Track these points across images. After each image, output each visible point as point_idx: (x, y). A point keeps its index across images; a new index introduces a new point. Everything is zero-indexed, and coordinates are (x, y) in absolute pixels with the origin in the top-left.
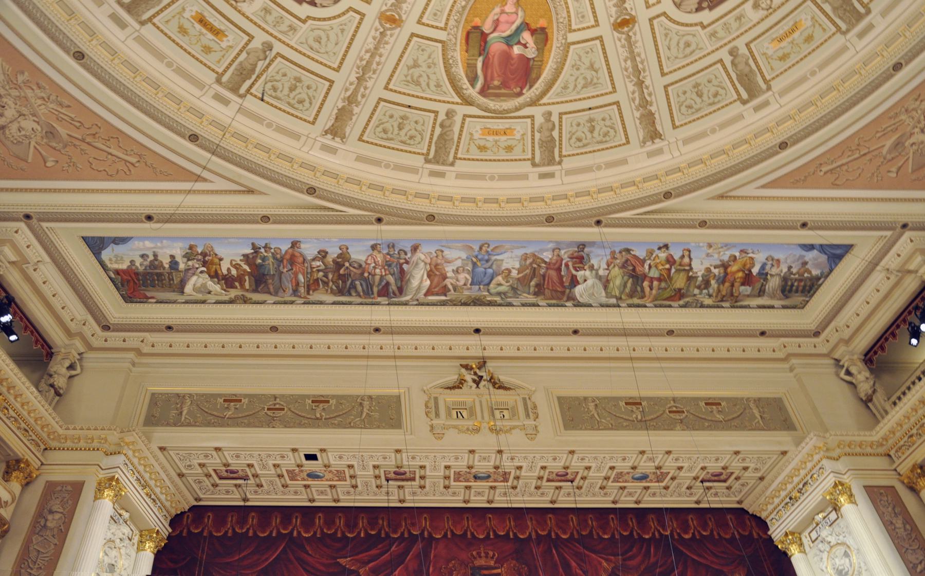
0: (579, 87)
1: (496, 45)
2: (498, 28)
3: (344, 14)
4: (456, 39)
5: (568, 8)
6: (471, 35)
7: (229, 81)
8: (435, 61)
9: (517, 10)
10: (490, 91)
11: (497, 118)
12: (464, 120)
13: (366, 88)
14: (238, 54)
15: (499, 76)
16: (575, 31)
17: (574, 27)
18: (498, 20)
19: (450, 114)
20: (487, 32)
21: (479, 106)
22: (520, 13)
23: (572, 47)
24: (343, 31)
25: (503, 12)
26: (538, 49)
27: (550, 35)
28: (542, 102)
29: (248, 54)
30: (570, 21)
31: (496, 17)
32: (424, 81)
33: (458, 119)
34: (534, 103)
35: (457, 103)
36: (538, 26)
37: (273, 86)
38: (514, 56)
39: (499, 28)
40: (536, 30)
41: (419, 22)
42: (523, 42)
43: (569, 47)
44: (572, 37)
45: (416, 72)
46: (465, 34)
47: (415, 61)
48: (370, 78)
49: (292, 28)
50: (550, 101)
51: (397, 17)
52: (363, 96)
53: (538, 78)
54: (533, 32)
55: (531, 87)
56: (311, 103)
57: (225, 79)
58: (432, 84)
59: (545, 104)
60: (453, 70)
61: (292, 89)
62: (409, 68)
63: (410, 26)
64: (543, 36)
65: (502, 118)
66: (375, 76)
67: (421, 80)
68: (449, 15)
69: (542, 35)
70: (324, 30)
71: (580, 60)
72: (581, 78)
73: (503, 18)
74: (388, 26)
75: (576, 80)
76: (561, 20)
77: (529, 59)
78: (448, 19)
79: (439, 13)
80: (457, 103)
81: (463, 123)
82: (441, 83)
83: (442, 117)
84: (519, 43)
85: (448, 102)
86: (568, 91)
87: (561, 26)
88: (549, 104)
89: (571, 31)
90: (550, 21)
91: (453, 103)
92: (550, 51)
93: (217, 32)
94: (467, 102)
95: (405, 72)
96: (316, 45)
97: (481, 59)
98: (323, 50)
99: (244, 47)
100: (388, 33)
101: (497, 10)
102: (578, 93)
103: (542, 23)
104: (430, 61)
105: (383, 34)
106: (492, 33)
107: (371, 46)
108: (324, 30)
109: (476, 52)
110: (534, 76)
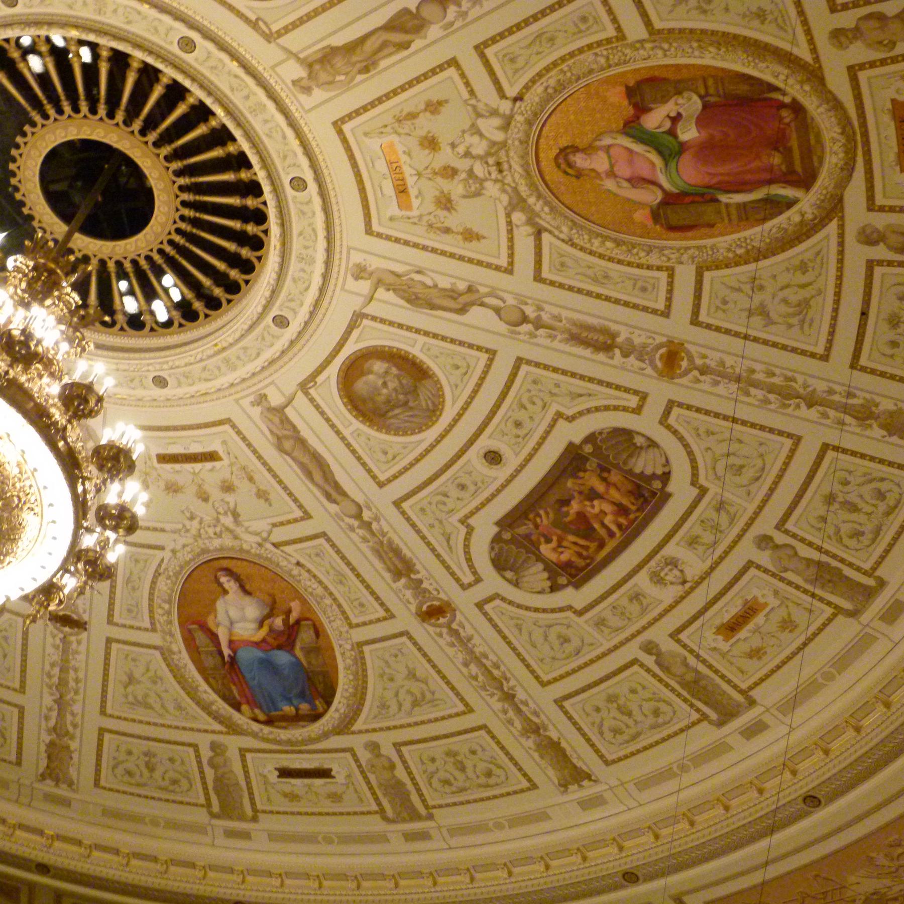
1: (689, 174)
3: (675, 432)
4: (687, 248)
5: (572, 55)
7: (851, 599)
8: (744, 278)
9: (600, 148)
10: (799, 169)
11: (866, 143)
12: (882, 209)
13: (831, 392)
14: (790, 583)
15: (758, 157)
16: (619, 29)
17: (611, 32)
18: (629, 180)
19: (870, 238)
20: (659, 196)
22: (607, 141)
23: (658, 24)
24: (709, 433)
26: (679, 93)
27: (644, 75)
28: (807, 57)
29: (786, 570)
30: (599, 44)
31: (626, 184)
32: (795, 296)
33: (880, 221)
34: (814, 75)
35: (841, 227)
36: (625, 102)
37: (851, 537)
38: (705, 135)
39: (646, 174)
40: (636, 106)
41: (666, 313)
42: (668, 124)
43: (660, 32)
44: (635, 30)
45: (776, 310)
46: (672, 235)
48: (805, 386)
49: (721, 506)
50: (802, 38)
51: (663, 350)
52: (849, 395)
54: (641, 109)
55: (776, 89)
56: (883, 480)
57: (847, 605)
58: (801, 278)
59: (814, 50)
61: (854, 508)
62: (769, 322)
63: (678, 327)
65: (865, 134)
66: (800, 379)
67: (794, 298)
68: (639, 266)
69: (643, 91)
70: (715, 461)
73: (624, 170)
74: (684, 364)
76: (602, 61)
77: (705, 106)
78: (649, 267)
79: (639, 284)
80: (841, 227)
81: (892, 209)
82: (796, 262)
83: (880, 252)
84: (672, 132)
85: (841, 244)
87: (614, 59)
88: (811, 41)
89: (621, 36)
91: (841, 235)
92: (678, 67)
93: (749, 611)
94: (834, 207)
96: (749, 473)
97: (724, 198)
98: (759, 463)
99: (774, 575)
101: (610, 184)
103: (617, 97)
105: (704, 370)
106: (660, 187)
107: (734, 387)
108: (715, 461)
109: (709, 209)
110: (743, 89)
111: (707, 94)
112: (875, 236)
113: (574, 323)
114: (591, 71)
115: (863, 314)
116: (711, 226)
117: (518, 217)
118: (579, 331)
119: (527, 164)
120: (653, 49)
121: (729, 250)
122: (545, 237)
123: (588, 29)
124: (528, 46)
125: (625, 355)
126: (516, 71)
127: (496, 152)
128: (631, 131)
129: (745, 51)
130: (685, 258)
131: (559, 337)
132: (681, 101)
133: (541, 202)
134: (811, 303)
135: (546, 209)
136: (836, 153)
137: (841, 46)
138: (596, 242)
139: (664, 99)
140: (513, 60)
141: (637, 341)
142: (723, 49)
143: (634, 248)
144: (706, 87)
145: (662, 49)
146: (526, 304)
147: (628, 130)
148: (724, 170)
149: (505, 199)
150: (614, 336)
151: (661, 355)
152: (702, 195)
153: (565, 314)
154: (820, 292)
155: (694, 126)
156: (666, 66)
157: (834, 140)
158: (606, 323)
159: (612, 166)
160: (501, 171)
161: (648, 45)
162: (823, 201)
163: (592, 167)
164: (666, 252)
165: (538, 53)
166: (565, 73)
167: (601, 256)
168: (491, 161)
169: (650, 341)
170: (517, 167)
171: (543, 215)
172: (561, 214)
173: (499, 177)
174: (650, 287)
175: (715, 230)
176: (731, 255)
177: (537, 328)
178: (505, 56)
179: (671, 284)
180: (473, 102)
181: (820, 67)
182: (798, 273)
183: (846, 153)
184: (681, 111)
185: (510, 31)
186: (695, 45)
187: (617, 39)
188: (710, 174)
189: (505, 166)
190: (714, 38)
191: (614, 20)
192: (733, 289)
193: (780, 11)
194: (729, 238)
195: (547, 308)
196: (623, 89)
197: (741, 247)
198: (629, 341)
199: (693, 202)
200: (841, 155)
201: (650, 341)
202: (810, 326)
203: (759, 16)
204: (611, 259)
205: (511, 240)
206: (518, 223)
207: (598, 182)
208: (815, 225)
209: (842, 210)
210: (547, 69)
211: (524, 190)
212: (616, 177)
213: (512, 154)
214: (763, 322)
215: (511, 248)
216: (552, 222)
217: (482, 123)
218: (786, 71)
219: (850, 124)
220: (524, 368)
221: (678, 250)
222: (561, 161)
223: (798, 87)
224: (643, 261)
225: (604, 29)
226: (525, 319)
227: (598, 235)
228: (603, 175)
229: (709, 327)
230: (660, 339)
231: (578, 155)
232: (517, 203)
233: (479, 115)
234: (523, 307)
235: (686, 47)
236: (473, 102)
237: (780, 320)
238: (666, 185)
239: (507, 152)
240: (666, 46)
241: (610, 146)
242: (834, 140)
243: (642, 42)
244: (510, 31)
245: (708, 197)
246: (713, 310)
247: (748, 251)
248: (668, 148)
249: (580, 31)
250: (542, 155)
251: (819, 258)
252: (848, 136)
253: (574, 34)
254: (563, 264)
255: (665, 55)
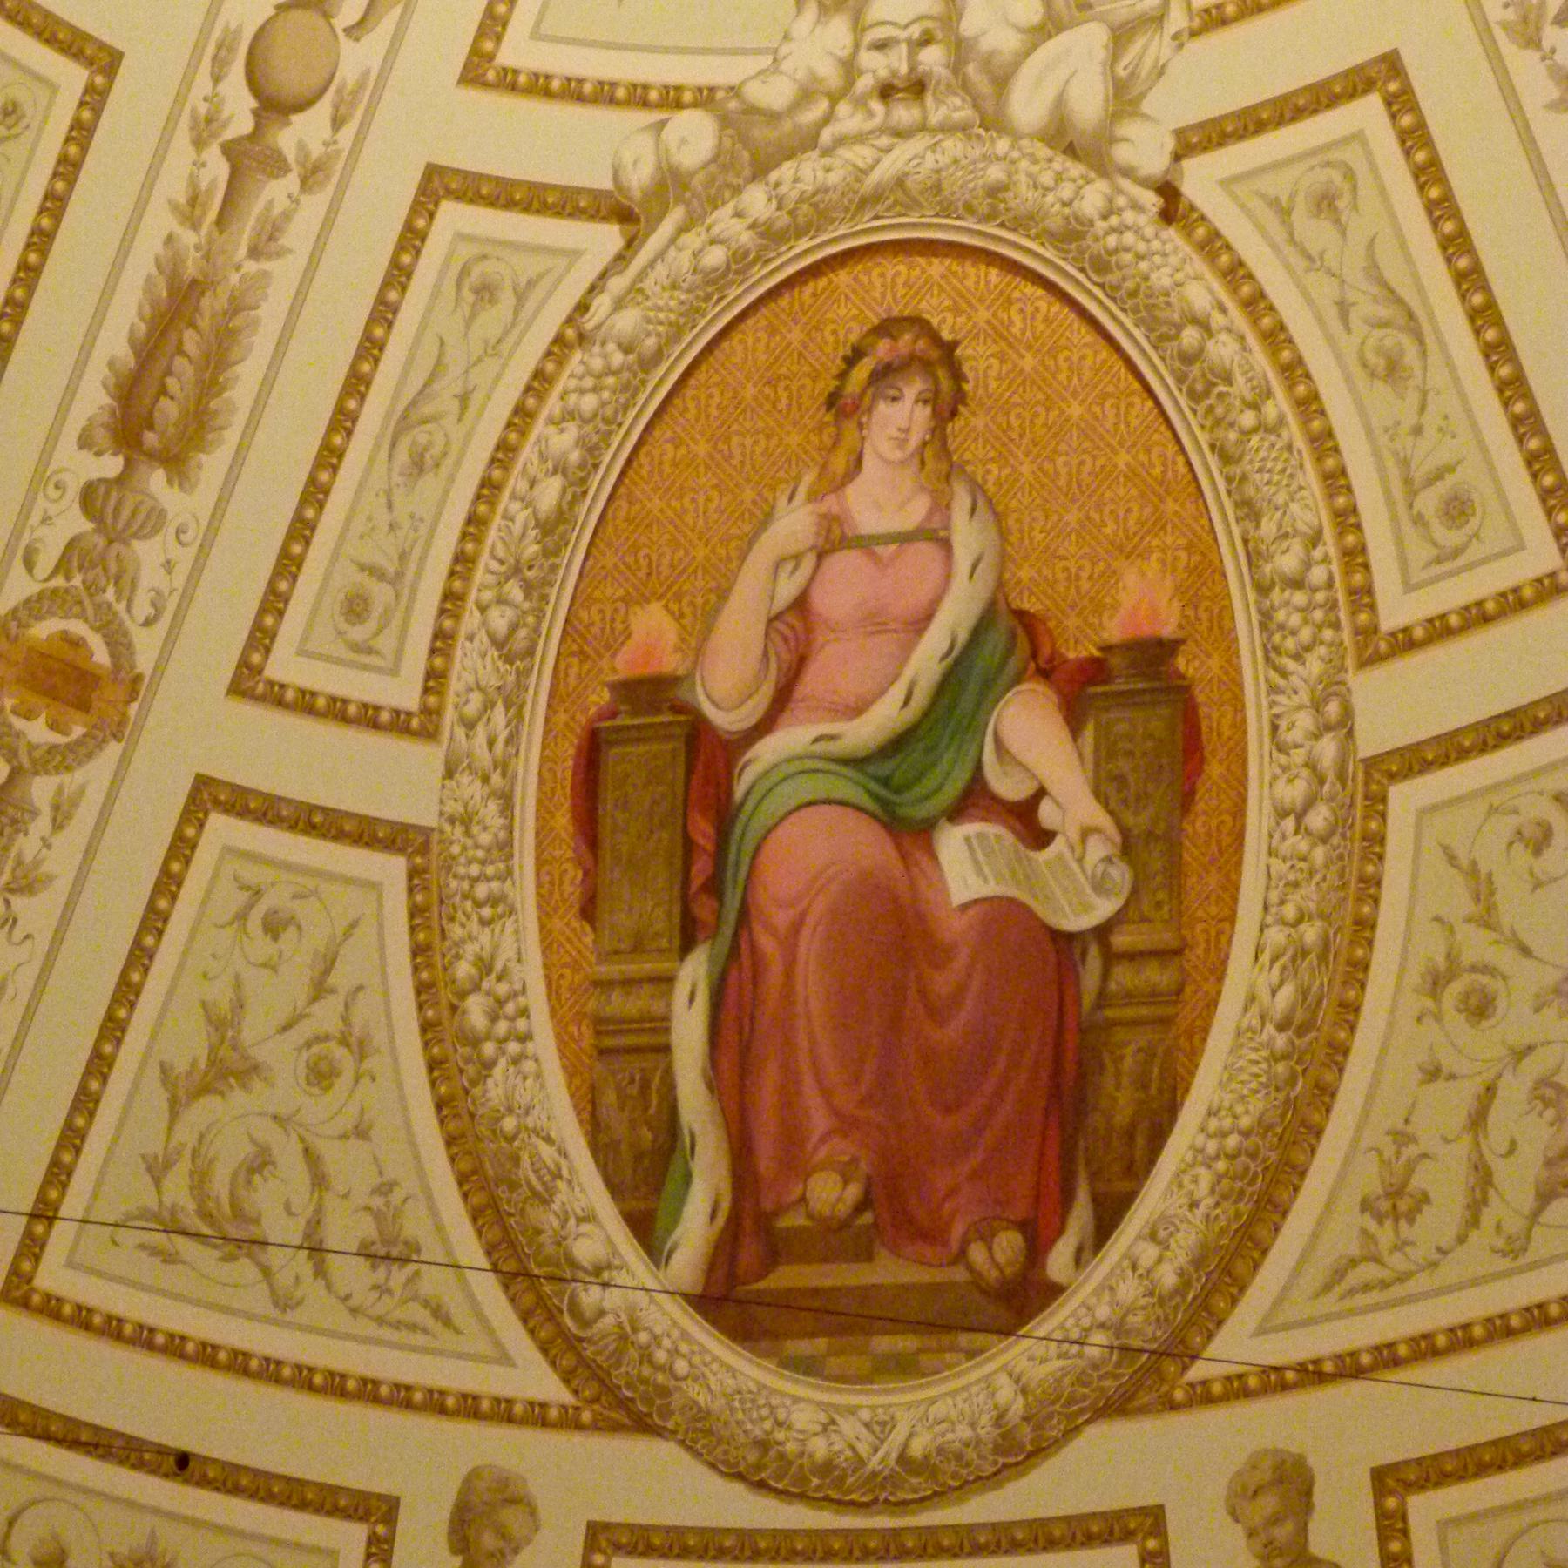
0: (1516, 1182)
1: (806, 851)
2: (812, 683)
4: (507, 801)
5: (1324, 442)
6: (616, 760)
9: (941, 506)
10: (787, 1277)
15: (846, 1125)
16: (1405, 643)
17: (1397, 609)
18: (801, 604)
20: (727, 721)
21: (704, 1438)
22: (969, 536)
23: (1405, 798)
25: (834, 538)
26: (1127, 847)
27: (1213, 718)
30: (1355, 557)
31: (787, 589)
32: (278, 1206)
34: (1149, 1373)
35: (537, 1416)
36: (1114, 631)
38: (953, 928)
40: (1095, 670)
41: (248, 682)
42: (1008, 787)
43: (1377, 802)
45: (230, 1123)
46: (568, 750)
47: (222, 1025)
51: (101, 656)
53: (1158, 1137)
54: (1080, 689)
60: (496, 1089)
63: (191, 724)
64: (1157, 721)
68: (452, 601)
71: (1486, 919)
72: (1515, 1090)
73: (844, 589)
74: (38, 731)
75: (1478, 1120)
76: (1288, 561)
77: (1064, 941)
78: (442, 641)
79: (381, 594)
80: (537, 1416)
82: (415, 1225)
84: (974, 799)
85: (469, 1408)
86: (1437, 1223)
87: (1289, 607)
88: (1275, 1381)
90: (1201, 580)
91: (504, 1412)
94: (616, 1395)
95: (150, 1135)
97: (695, 971)
100: (42, 790)
101: (794, 523)
102: (1515, 1248)
103: (1141, 601)
104: (326, 1017)
106: (766, 725)
109: (661, 917)
110: (1119, 1100)
111: (1111, 958)
112: (489, 1541)
113: (237, 306)
114: (1250, 511)
115: (184, 1460)
116: (588, 910)
117: (694, 138)
118: (204, 323)
119: (912, 204)
120: (1311, 765)
121: (485, 966)
122: (609, 237)
123: (1419, 520)
124: (1373, 270)
125: (89, 498)
126: (1283, 212)
127: (966, 86)
128: (996, 639)
129: (1262, 1126)
130: (468, 786)
131: (189, 238)
132: (1097, 850)
133: (746, 238)
134: (245, 1269)
135: (715, 257)
136: (827, 1427)
137: (1241, 1496)
138: (563, 442)
139: (1108, 786)
140: (1325, 203)
141: (148, 554)
142: (1281, 1041)
143: (528, 588)
144: (1133, 956)
145: (1310, 803)
146: (337, 123)
147: (1005, 621)
148: (809, 985)
149: (774, 94)
150: (175, 462)
151: (77, 643)
152: (714, 887)
153: (284, 273)
154: (284, 1302)
155: (991, 889)
156: (1239, 812)
157: (881, 1427)
158: (232, 436)
159: (866, 544)
160: (886, 92)
161: (1327, 749)
162: (646, 1357)
163: (869, 461)
164: (499, 715)
165: (1343, 308)
166: (1255, 406)
167: (505, 452)
168: (932, 57)
169: (142, 608)
170: (898, 159)
171: (692, 240)
172: (692, 313)
173: (865, 83)
174: (358, 633)
175: (568, 921)
176: (464, 970)
177: (231, 151)
178: (1349, 174)
179: (369, 718)
180: (1177, 20)
181: (1173, 1407)
182: (366, 1228)
183: (826, 1468)
184: (1058, 845)
185: (1442, 207)
186: (1311, 933)
187: (1367, 633)
188: (797, 926)
189: (904, 114)
190: (1326, 1013)
191: (1440, 630)
192: (328, 963)
193: (1402, 1278)
194: (533, 974)
195: (314, 207)
196: (1168, 631)
197: (494, 1018)
198: (154, 520)
199: (689, 845)
200: (819, 1448)
201: (142, 608)
202: (154, 1251)
203: (1396, 1192)
204: (489, 489)
205: (605, 95)
206: (671, 134)
207: (809, 478)
208: (552, 1317)
209: (600, 1426)
210: (1276, 337)
211: (803, 175)
212: (821, 556)
213: (953, 146)
214: (181, 1066)
215: (574, 92)
216: (661, 270)
217: (1086, 43)
218: (1168, 1278)
219: (937, 1497)
220: (72, 77)
221: (503, 766)
222: (906, 341)
223: (1103, 1312)
224: (471, 619)
225: (1409, 587)
226: (274, 107)
227: (592, 451)
228: (830, 504)
229: (182, 848)
230: (146, 648)
231: (923, 413)
232: (756, 142)
233: (1121, 35)
234: (322, 111)
235: (1308, 896)
236: (1177, 20)
237: (185, 1135)
238: (767, 751)
239: (964, 128)
240: (1318, 819)
241: (946, 545)
242: (881, 1427)
243: (1345, 725)
244: (1442, 207)
245: (703, 909)
246: (252, 874)
247: (475, 1042)
248: (915, 780)
249: (1412, 491)
250: (937, 267)
251: (421, 1315)
252: (891, 1480)
253: (1405, 463)
254: (486, 292)
255: (1282, 813)
